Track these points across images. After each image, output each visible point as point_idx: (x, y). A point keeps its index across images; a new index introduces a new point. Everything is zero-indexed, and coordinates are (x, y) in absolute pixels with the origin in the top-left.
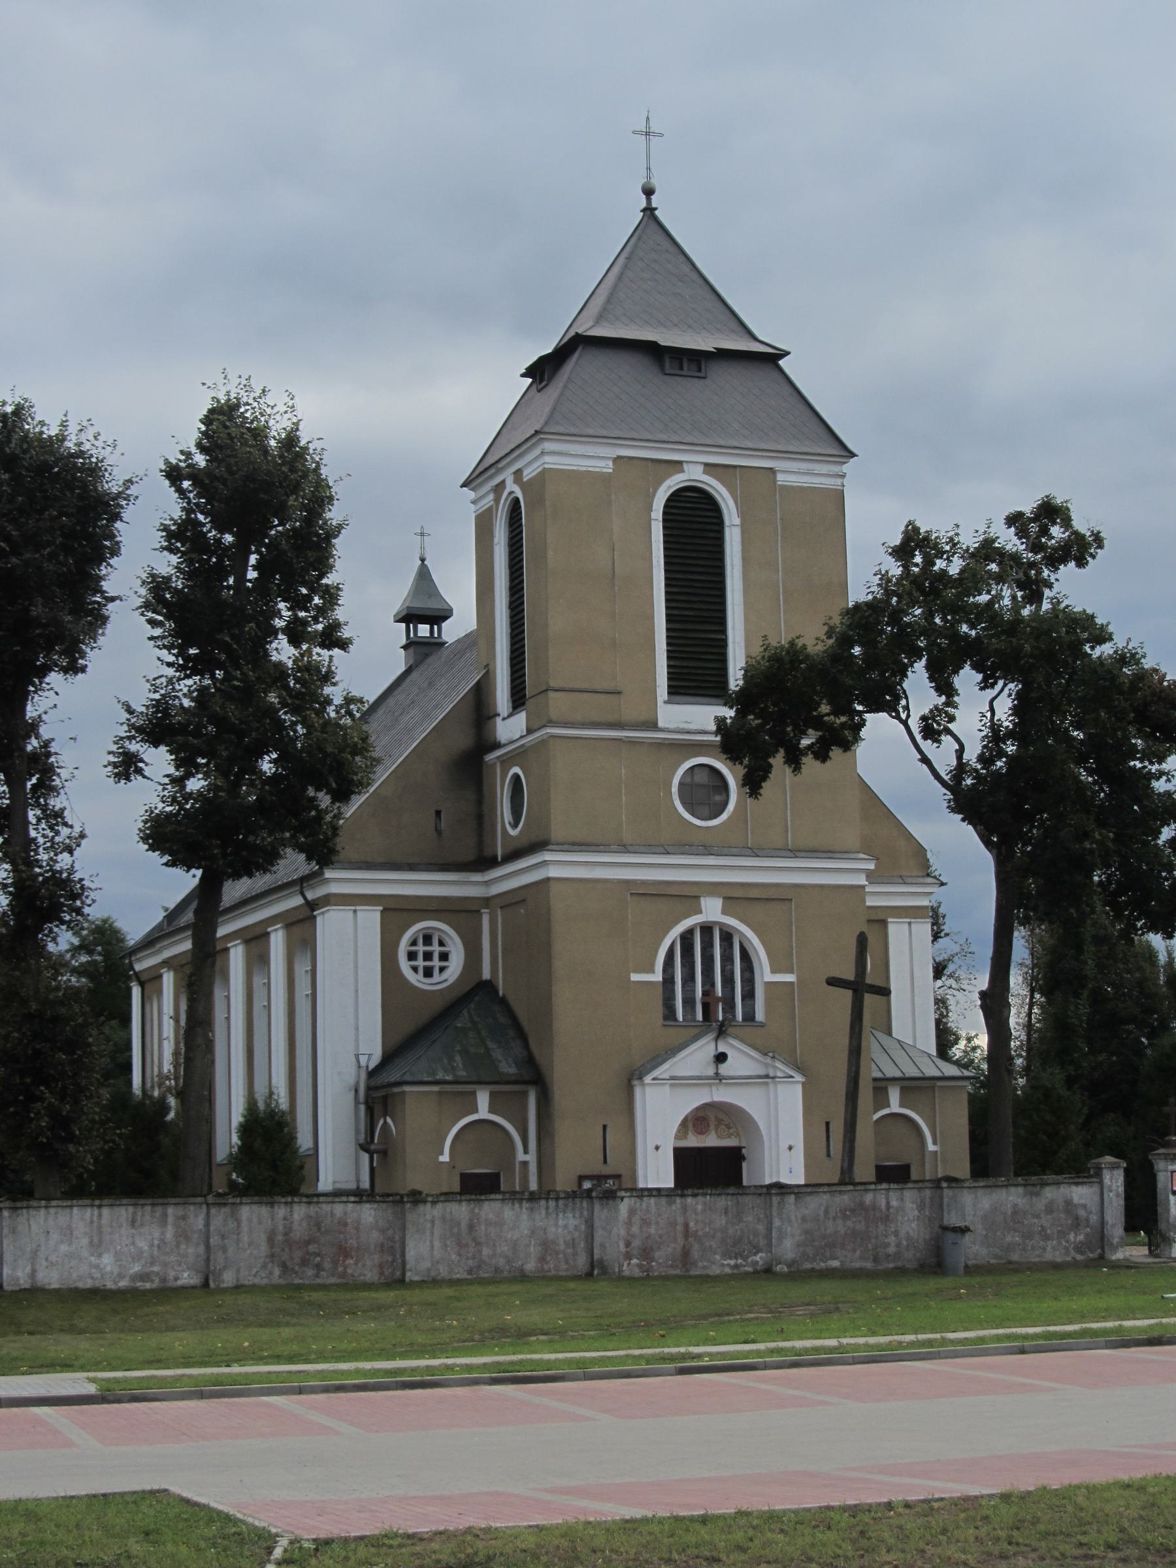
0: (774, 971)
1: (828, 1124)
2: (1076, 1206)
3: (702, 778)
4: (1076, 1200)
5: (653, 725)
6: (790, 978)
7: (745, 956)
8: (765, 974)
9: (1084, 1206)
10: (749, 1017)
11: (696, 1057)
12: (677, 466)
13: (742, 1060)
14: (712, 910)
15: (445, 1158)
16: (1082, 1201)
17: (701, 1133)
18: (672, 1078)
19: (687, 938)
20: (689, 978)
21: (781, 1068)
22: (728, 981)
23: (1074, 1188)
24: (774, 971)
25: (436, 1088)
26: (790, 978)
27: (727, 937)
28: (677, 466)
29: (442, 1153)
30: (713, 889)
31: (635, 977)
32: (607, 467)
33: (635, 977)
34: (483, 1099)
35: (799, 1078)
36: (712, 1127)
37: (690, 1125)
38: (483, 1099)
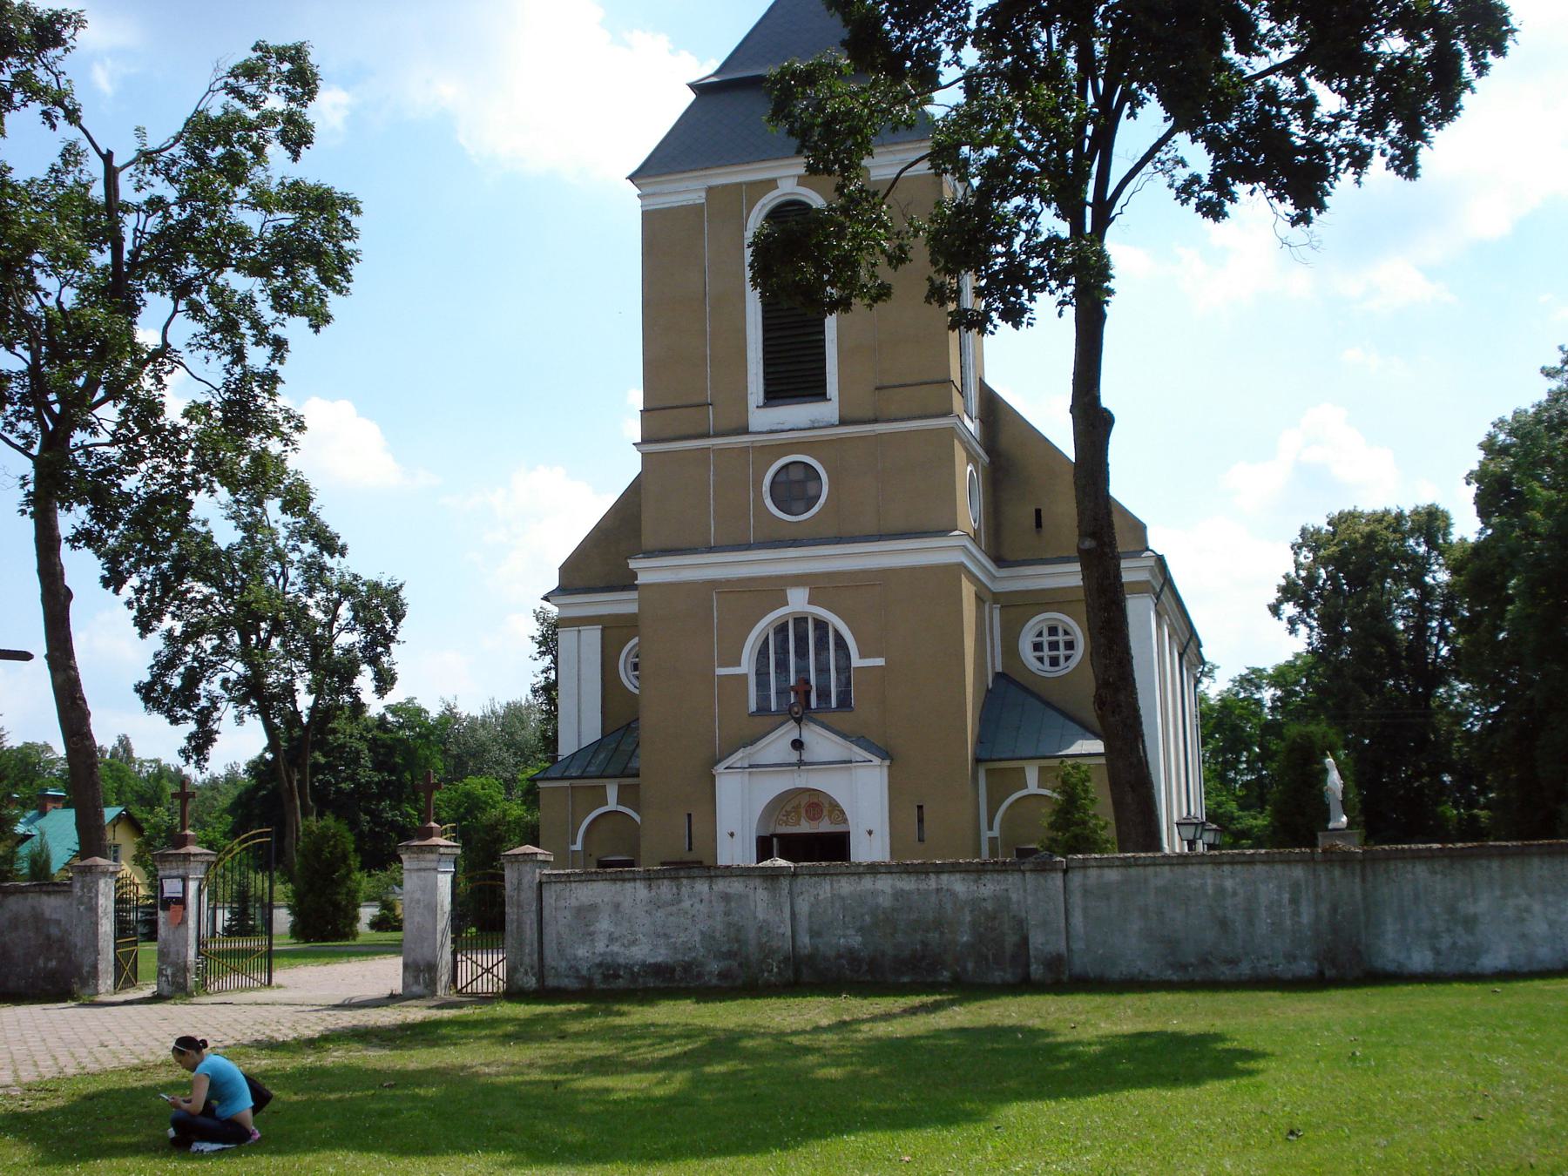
0: (862, 656)
1: (920, 807)
2: (48, 921)
3: (796, 474)
4: (47, 914)
5: (745, 430)
6: (880, 662)
7: (841, 643)
8: (856, 662)
9: (58, 922)
10: (844, 702)
11: (776, 746)
12: (771, 184)
13: (822, 743)
14: (798, 601)
15: (578, 846)
16: (55, 916)
17: (814, 819)
18: (751, 766)
19: (781, 629)
20: (782, 665)
21: (859, 753)
22: (823, 670)
23: (45, 898)
24: (862, 656)
25: (566, 783)
26: (880, 662)
27: (821, 625)
28: (771, 184)
29: (574, 843)
30: (798, 580)
31: (720, 671)
32: (698, 197)
33: (720, 671)
34: (612, 792)
35: (877, 761)
36: (825, 812)
37: (803, 812)
38: (612, 792)
